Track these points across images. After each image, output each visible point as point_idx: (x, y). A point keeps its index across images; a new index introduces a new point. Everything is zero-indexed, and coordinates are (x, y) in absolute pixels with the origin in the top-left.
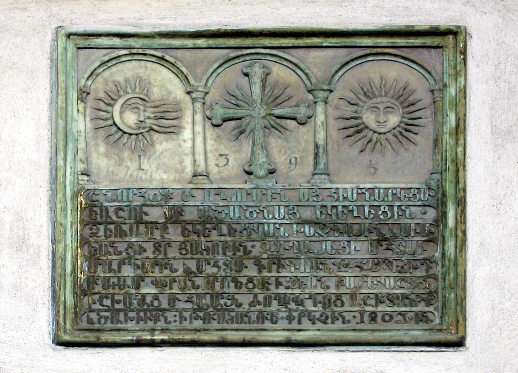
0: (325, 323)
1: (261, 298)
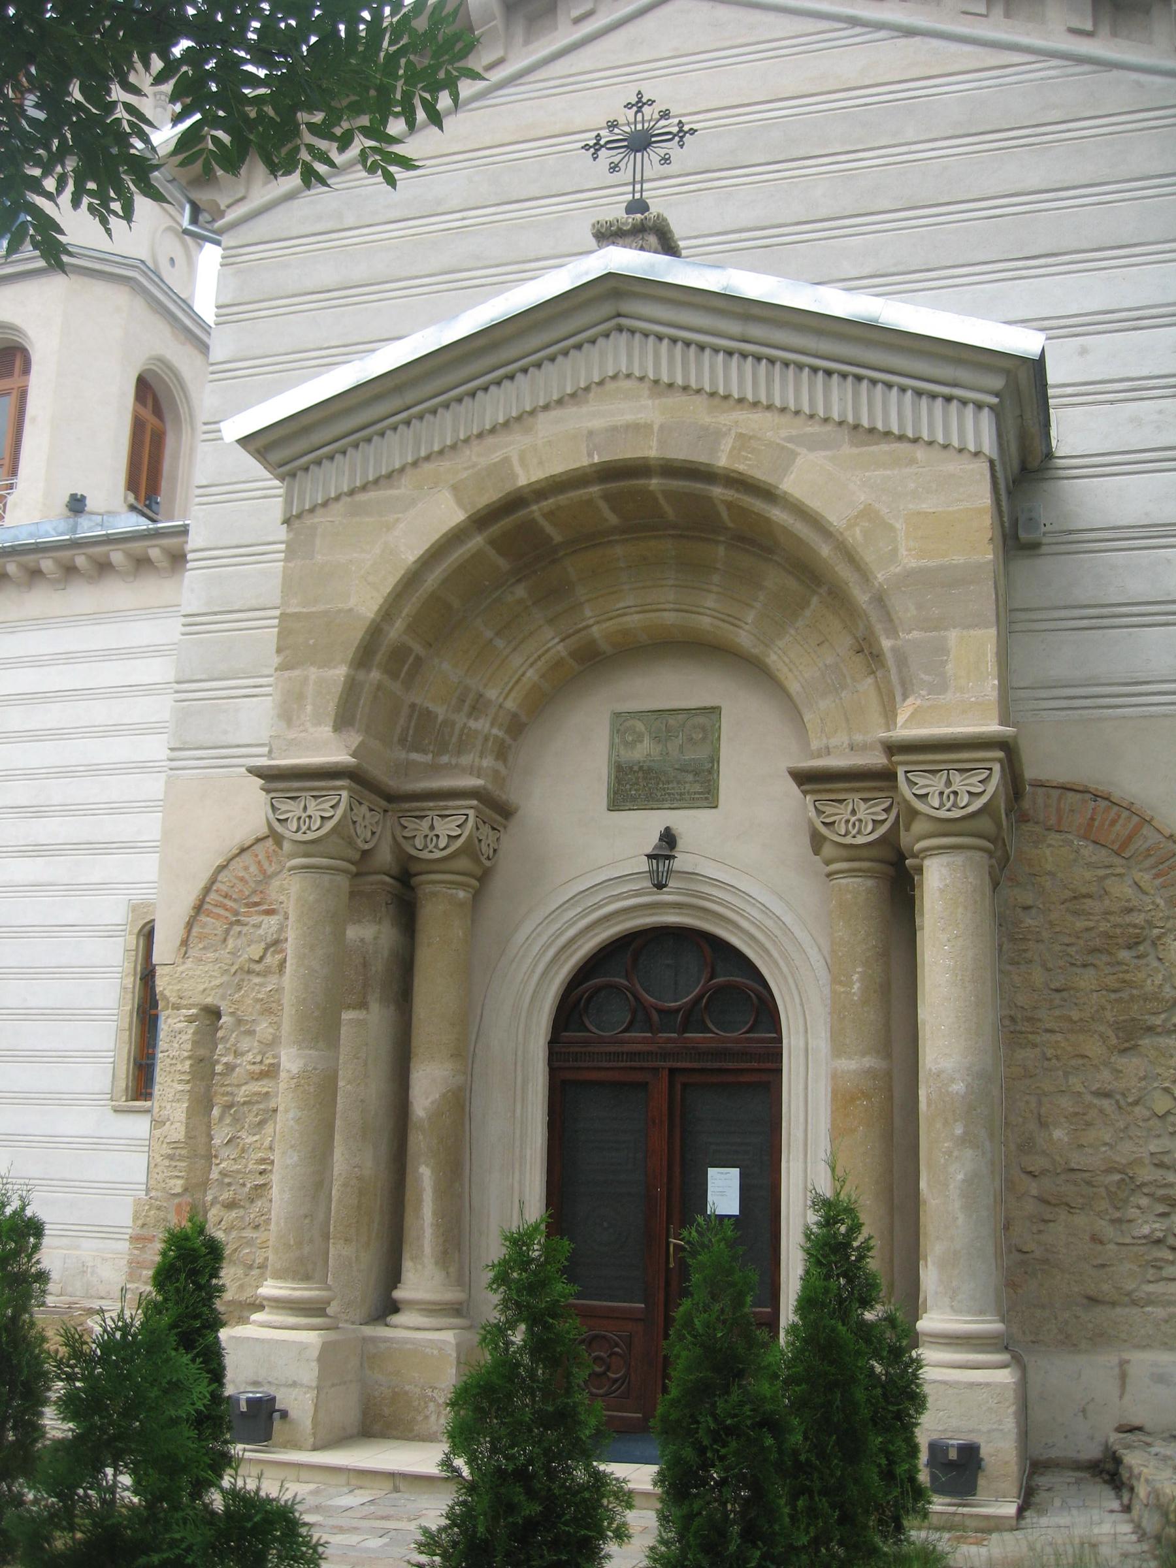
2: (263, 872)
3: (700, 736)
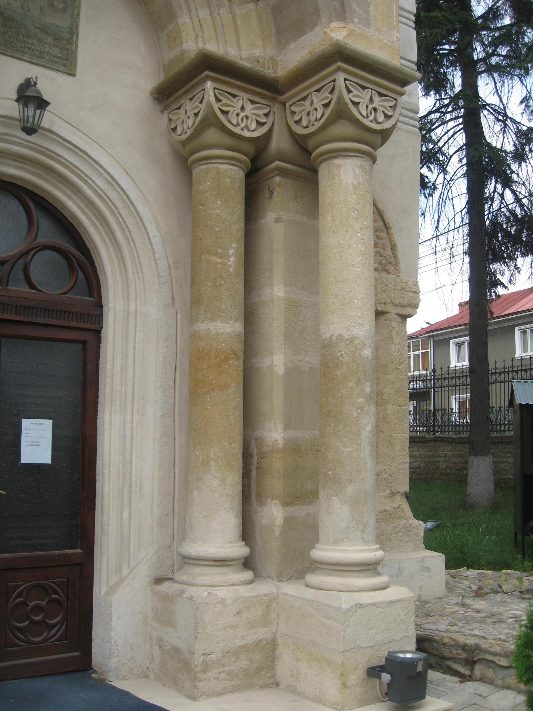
0: (40, 58)
1: (23, 46)
3: (62, 6)
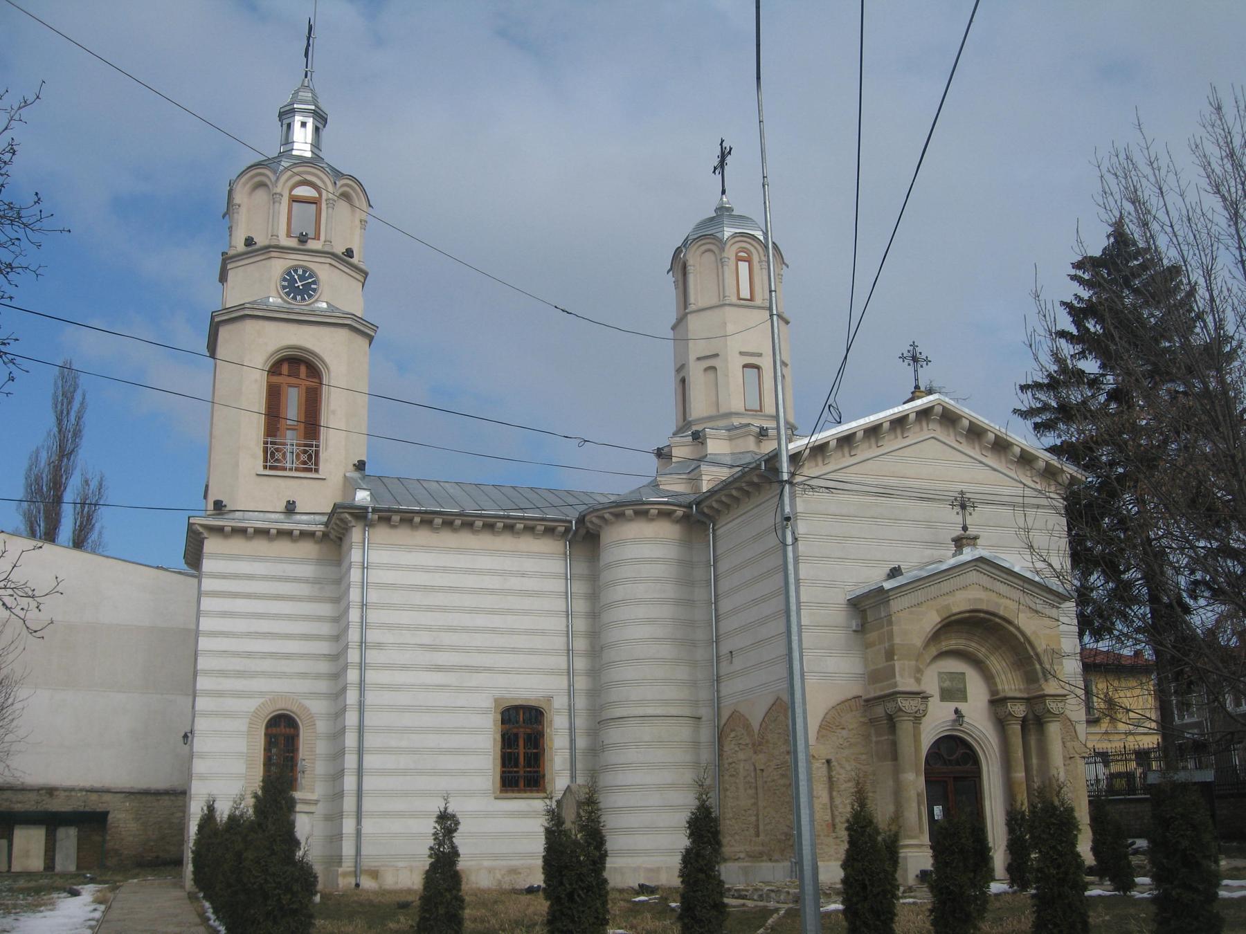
2: (840, 715)
